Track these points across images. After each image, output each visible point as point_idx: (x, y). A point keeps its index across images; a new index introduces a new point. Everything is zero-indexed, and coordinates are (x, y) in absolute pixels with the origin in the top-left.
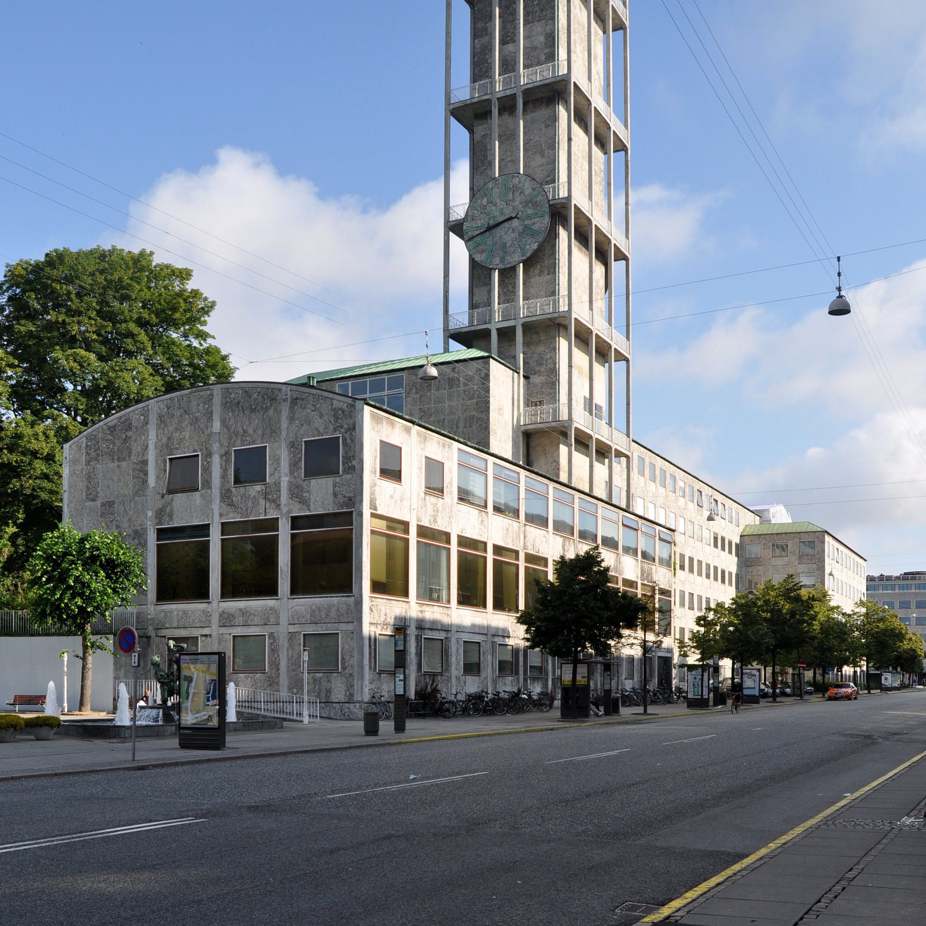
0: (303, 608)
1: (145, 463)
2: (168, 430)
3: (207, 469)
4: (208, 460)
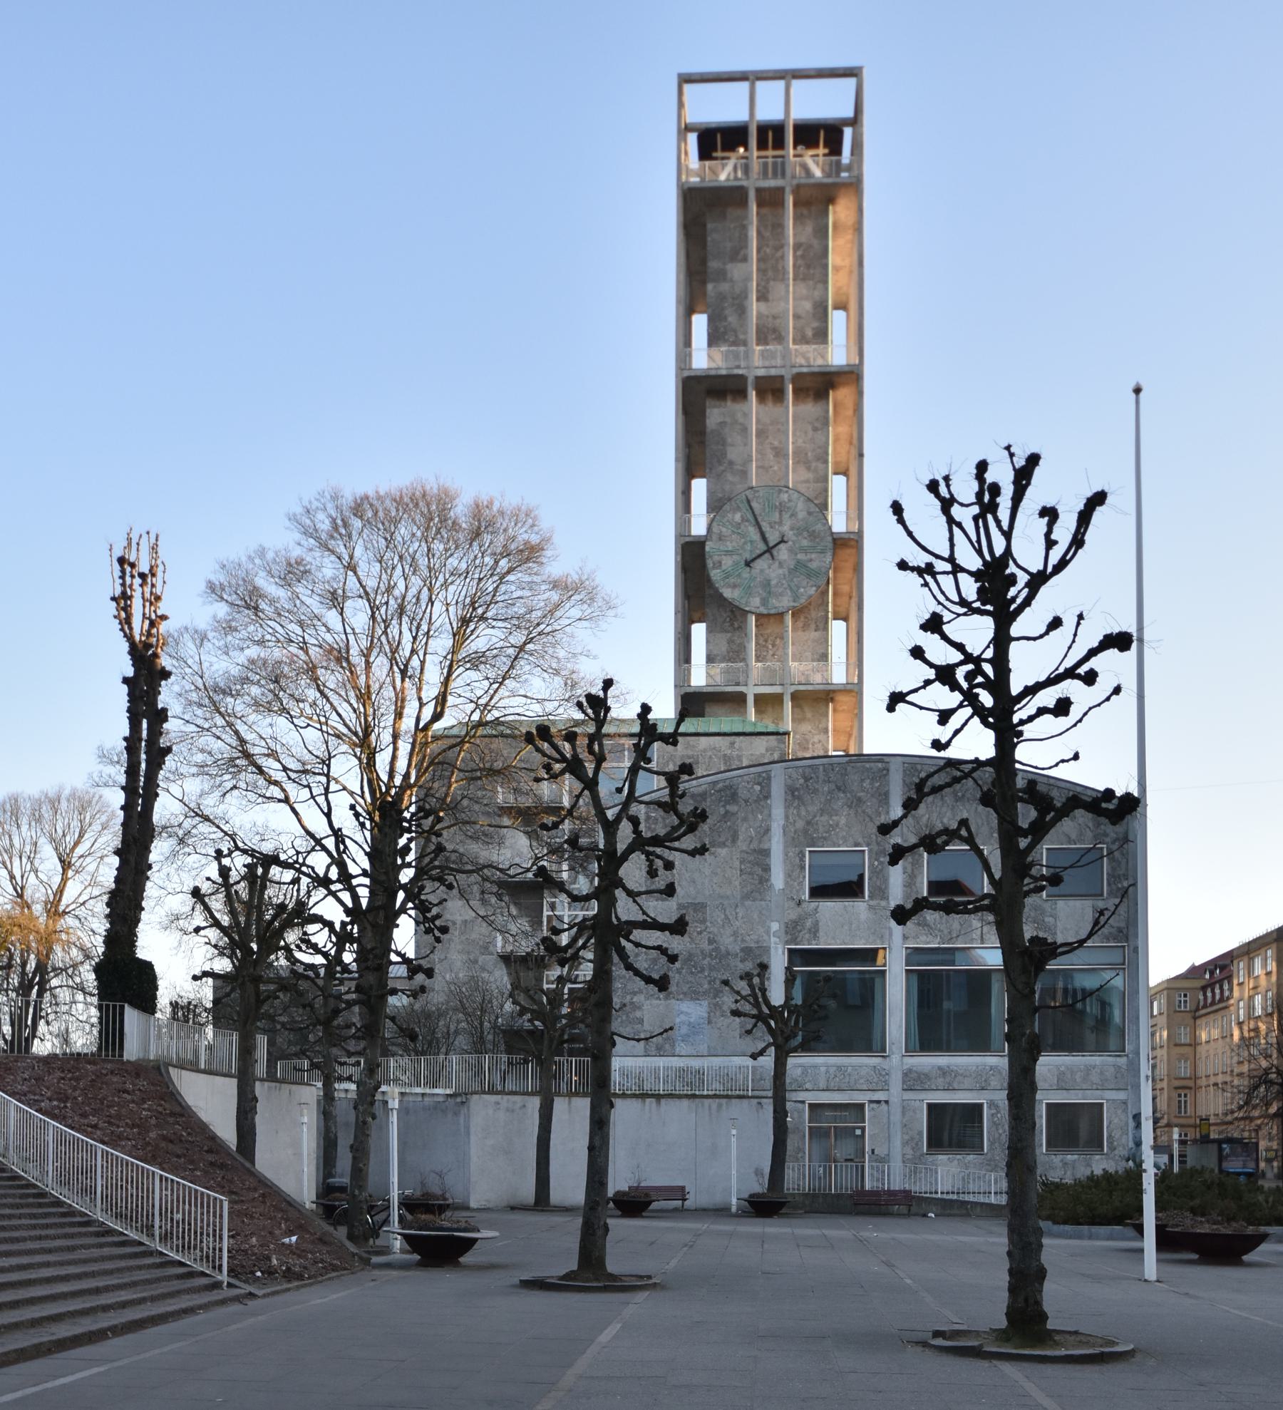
1: (766, 853)
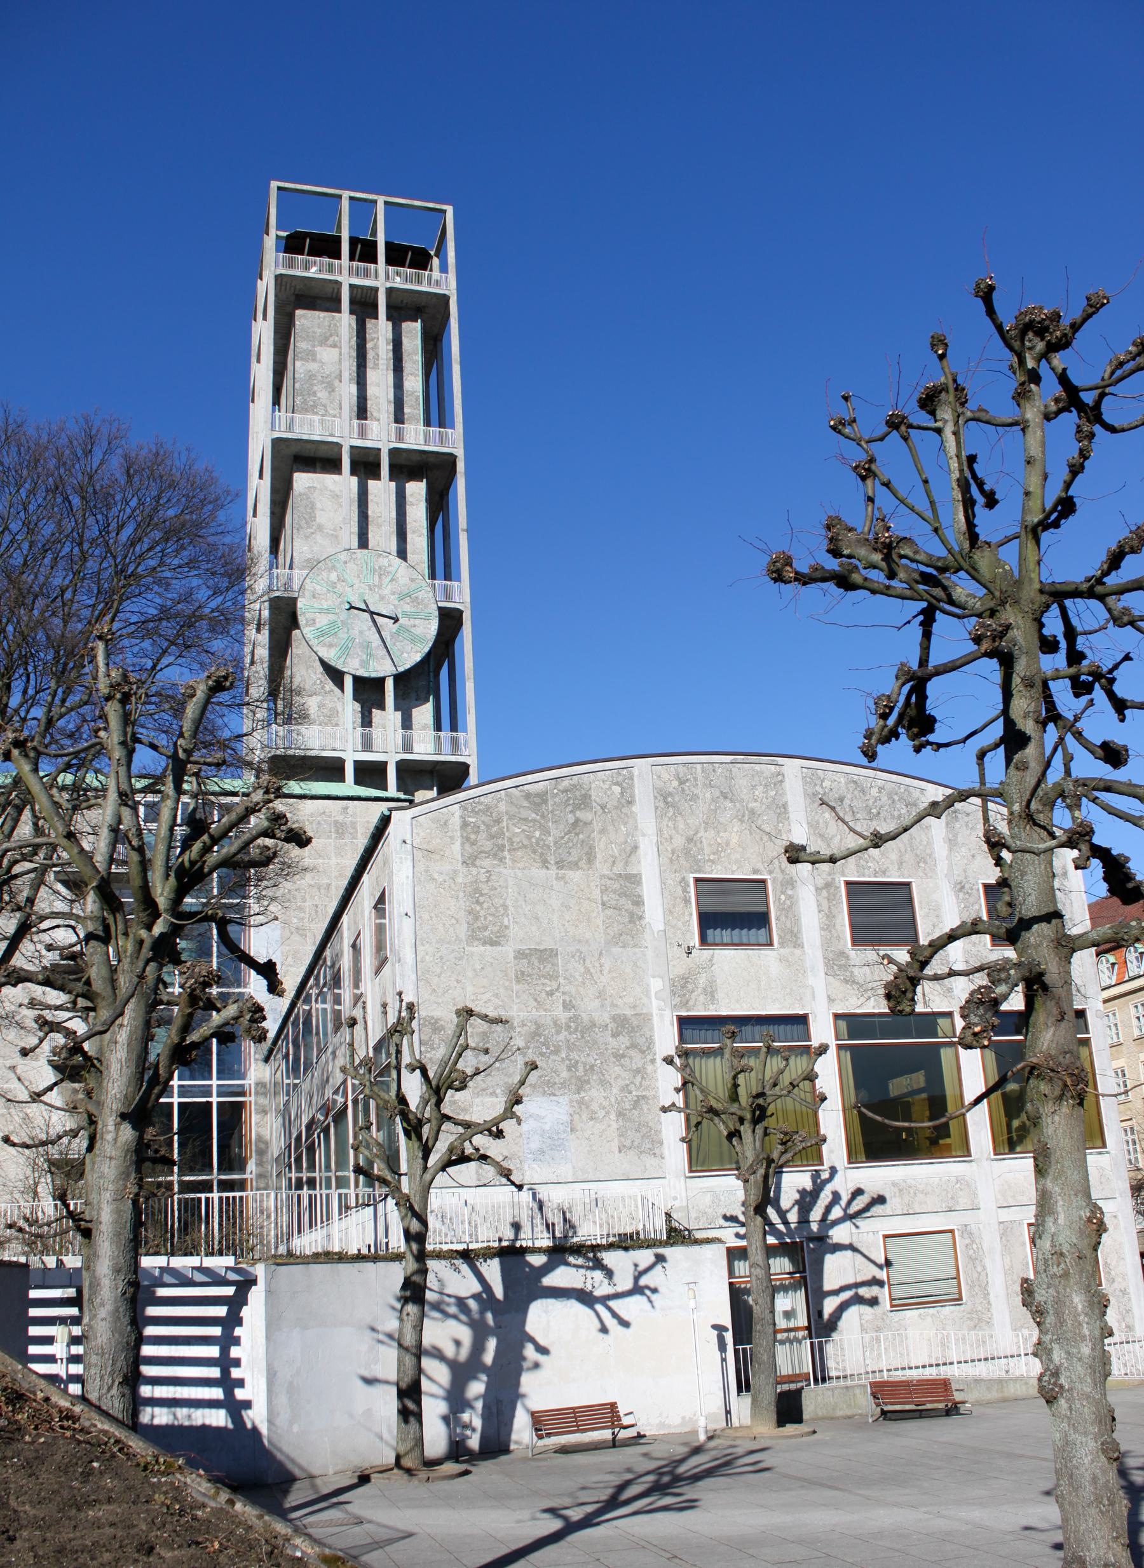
1: (634, 879)
4: (790, 892)
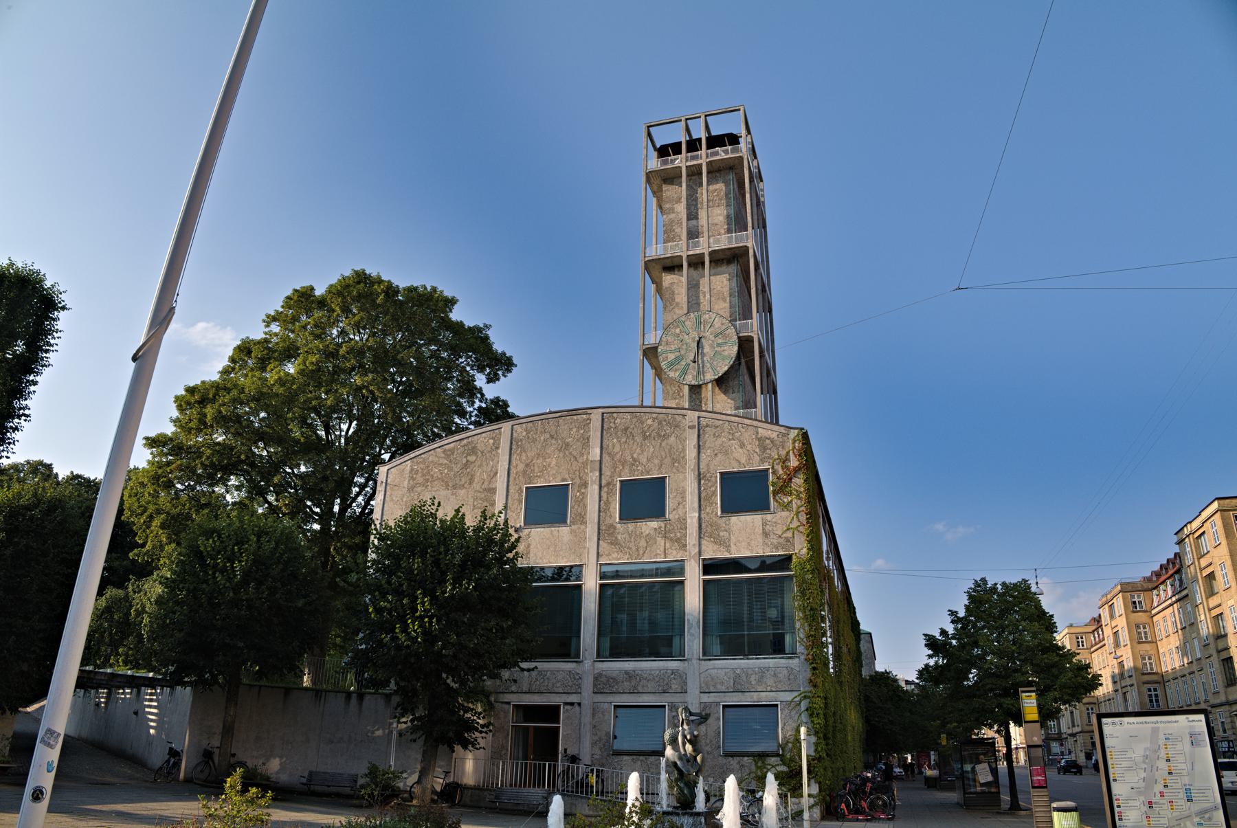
0: (722, 673)
1: (493, 491)
2: (527, 456)
3: (581, 501)
4: (583, 491)
